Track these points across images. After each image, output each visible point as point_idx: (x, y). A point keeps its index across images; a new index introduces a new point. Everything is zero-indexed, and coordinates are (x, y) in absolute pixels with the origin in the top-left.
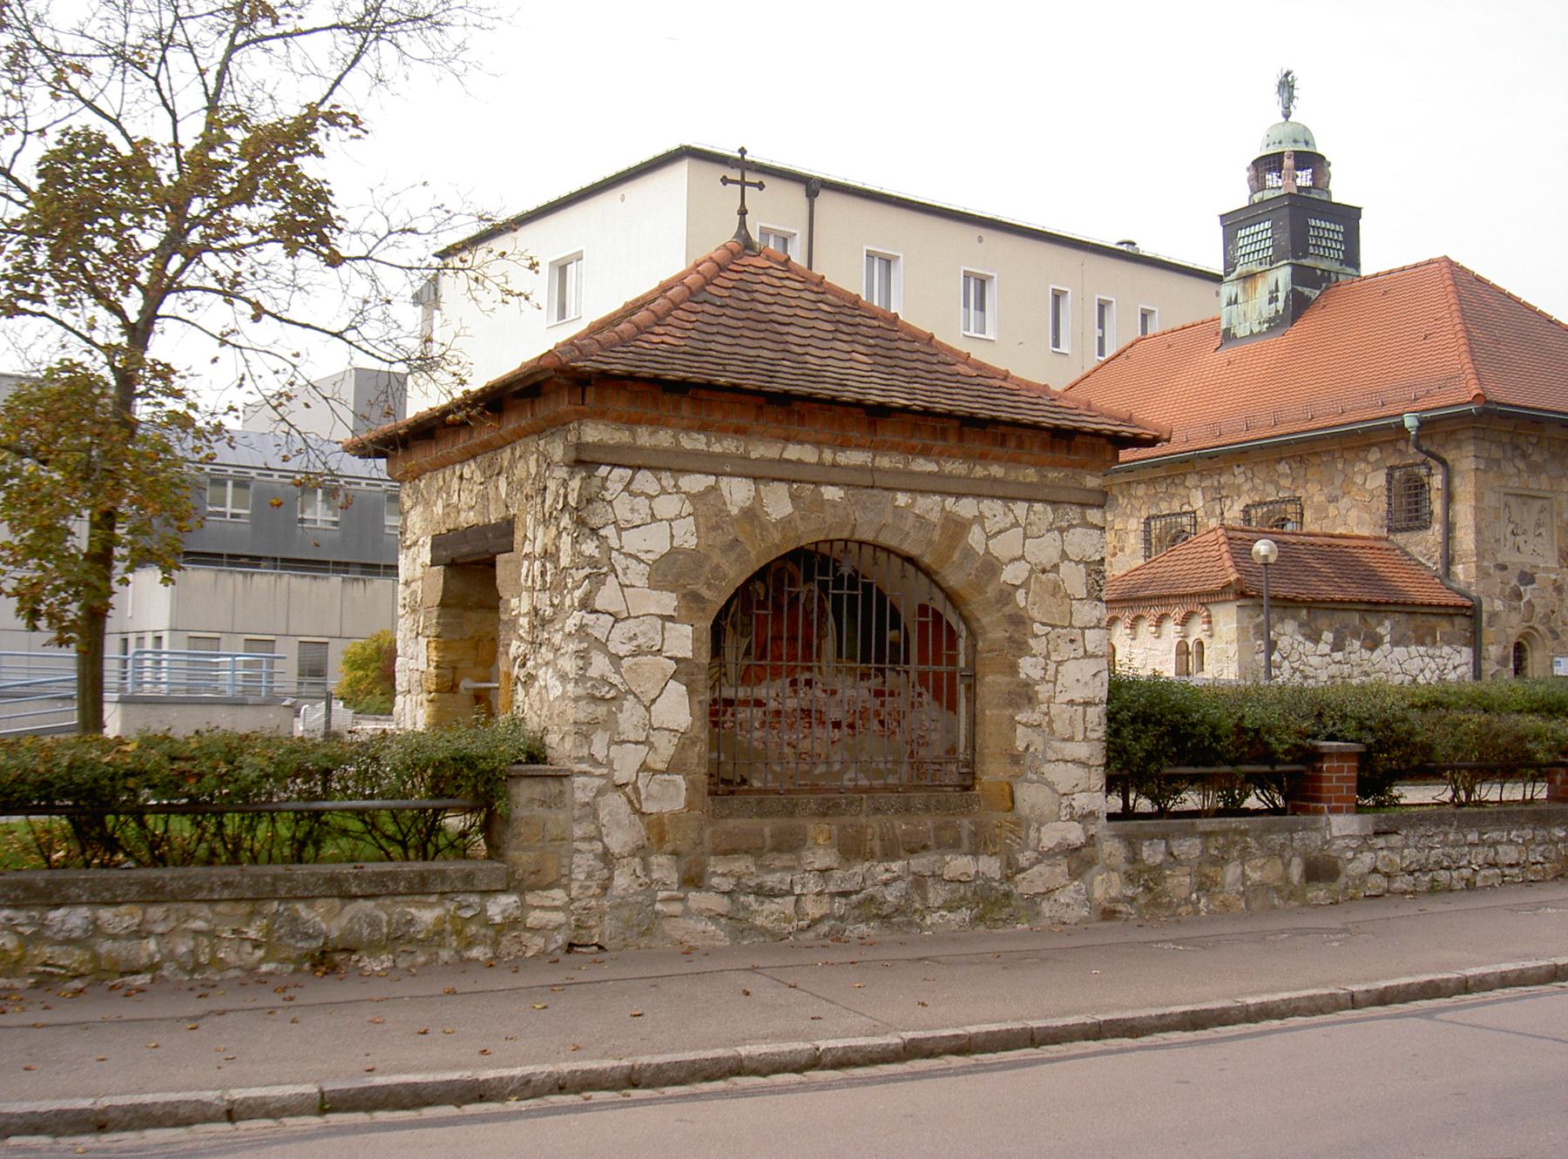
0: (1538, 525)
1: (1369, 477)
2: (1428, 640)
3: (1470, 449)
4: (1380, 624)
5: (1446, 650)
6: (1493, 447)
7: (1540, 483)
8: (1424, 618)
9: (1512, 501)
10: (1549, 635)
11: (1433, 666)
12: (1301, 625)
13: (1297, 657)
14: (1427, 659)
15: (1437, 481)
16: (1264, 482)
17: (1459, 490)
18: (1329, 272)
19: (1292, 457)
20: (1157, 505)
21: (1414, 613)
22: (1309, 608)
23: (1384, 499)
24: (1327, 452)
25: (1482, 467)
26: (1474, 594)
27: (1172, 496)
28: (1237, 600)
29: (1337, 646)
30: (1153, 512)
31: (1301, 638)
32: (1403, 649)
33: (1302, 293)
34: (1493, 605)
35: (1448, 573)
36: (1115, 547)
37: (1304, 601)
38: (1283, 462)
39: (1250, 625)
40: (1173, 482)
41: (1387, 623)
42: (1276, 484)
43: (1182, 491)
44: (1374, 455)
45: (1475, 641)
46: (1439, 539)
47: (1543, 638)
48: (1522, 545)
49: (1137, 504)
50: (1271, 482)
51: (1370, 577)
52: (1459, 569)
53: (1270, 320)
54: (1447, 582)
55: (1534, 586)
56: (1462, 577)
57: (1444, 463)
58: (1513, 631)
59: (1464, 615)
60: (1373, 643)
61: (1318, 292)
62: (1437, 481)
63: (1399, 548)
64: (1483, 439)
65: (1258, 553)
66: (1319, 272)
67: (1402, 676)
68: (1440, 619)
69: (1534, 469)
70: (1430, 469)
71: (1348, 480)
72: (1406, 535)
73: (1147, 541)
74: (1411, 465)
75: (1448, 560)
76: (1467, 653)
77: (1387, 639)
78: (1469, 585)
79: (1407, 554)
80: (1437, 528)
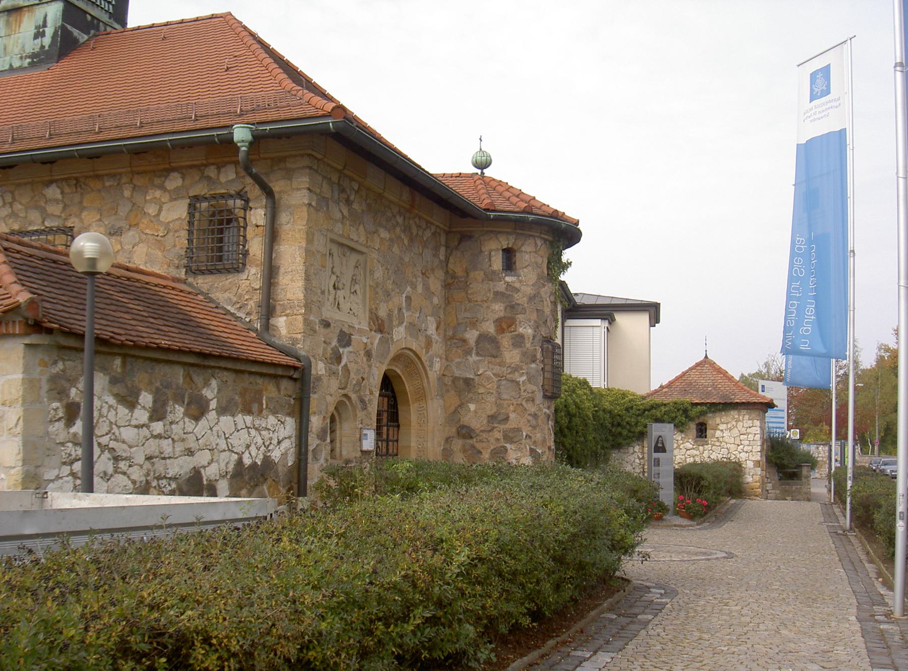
0: (354, 281)
1: (165, 207)
2: (255, 407)
3: (303, 180)
4: (207, 384)
5: (272, 420)
6: (325, 185)
7: (358, 236)
8: (252, 379)
9: (335, 249)
10: (359, 405)
11: (260, 441)
12: (114, 381)
13: (106, 429)
14: (253, 432)
15: (258, 216)
16: (27, 208)
17: (286, 228)
18: (99, 20)
21: (242, 372)
22: (124, 356)
23: (184, 234)
24: (113, 176)
25: (314, 204)
26: (303, 353)
28: (27, 334)
29: (157, 414)
31: (112, 401)
32: (229, 417)
33: (71, 33)
34: (319, 368)
35: (267, 326)
37: (122, 345)
38: (54, 185)
39: (43, 376)
41: (214, 383)
44: (174, 182)
45: (301, 412)
46: (257, 285)
47: (354, 408)
48: (341, 300)
50: (37, 207)
51: (186, 323)
52: (281, 322)
53: (33, 56)
54: (267, 337)
55: (350, 349)
56: (284, 332)
57: (269, 193)
59: (291, 378)
60: (198, 410)
61: (86, 37)
62: (258, 216)
63: (202, 293)
64: (316, 171)
65: (80, 253)
66: (89, 18)
67: (227, 453)
68: (267, 381)
69: (355, 219)
70: (247, 201)
71: (137, 209)
72: (210, 279)
74: (222, 196)
75: (269, 310)
76: (290, 424)
77: (213, 404)
78: (295, 341)
79: (211, 300)
80: (253, 276)
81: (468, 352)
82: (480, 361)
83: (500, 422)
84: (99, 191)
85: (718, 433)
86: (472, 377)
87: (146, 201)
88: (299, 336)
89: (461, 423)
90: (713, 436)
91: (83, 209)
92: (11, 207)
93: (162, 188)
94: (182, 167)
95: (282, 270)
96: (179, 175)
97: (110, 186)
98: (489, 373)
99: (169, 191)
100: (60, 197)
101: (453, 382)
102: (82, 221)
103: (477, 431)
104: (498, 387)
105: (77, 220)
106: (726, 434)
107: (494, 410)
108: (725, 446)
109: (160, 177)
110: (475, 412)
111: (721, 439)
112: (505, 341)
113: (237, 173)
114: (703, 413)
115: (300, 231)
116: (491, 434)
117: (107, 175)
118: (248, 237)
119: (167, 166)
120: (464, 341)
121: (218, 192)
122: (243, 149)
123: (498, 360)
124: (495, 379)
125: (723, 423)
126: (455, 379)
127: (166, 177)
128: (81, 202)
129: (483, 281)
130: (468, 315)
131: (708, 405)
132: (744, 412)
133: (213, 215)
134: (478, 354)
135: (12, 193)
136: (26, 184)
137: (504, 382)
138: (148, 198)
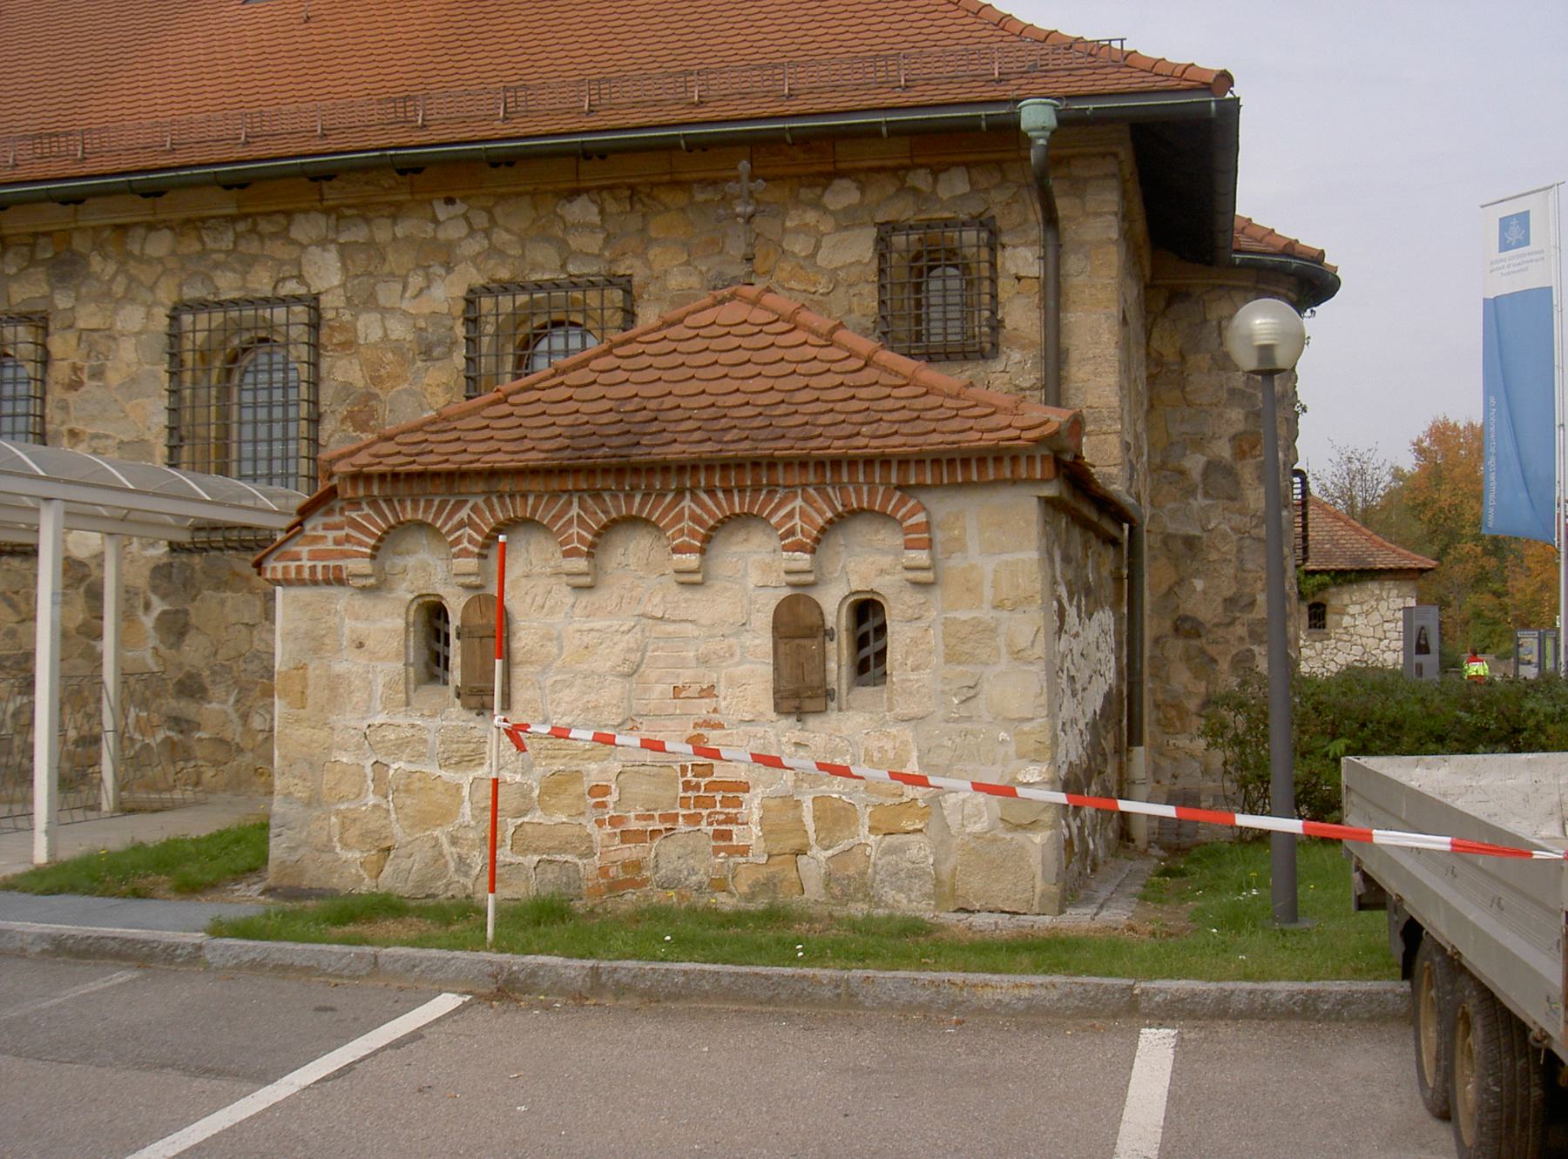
1: (826, 241)
16: (523, 240)
17: (1075, 281)
19: (610, 188)
20: (207, 278)
27: (249, 262)
30: (194, 292)
36: (76, 369)
38: (585, 197)
40: (253, 230)
42: (562, 245)
43: (279, 249)
44: (843, 195)
49: (145, 274)
50: (549, 239)
57: (1051, 220)
70: (994, 234)
73: (175, 357)
74: (947, 224)
81: (1190, 492)
82: (1212, 506)
83: (1242, 610)
84: (682, 210)
85: (1347, 621)
86: (1198, 533)
87: (784, 230)
88: (1114, 470)
89: (1181, 612)
90: (1339, 625)
91: (649, 242)
92: (487, 233)
93: (817, 205)
94: (858, 170)
95: (1074, 355)
96: (854, 185)
97: (706, 202)
98: (1225, 527)
99: (833, 213)
100: (597, 220)
101: (1165, 543)
102: (648, 264)
103: (1208, 626)
104: (1240, 550)
105: (637, 263)
106: (1360, 621)
107: (1234, 589)
108: (1359, 642)
109: (810, 186)
110: (1204, 592)
111: (1352, 630)
112: (1247, 471)
113: (972, 183)
114: (1322, 587)
115: (1105, 287)
116: (1231, 629)
117: (700, 181)
118: (1002, 296)
119: (830, 168)
120: (1182, 473)
121: (935, 216)
122: (1042, 142)
123: (1237, 505)
124: (1235, 538)
125: (1354, 603)
126: (1167, 539)
127: (825, 188)
128: (643, 230)
129: (1209, 370)
130: (1186, 428)
131: (1333, 574)
132: (1389, 584)
133: (917, 257)
134: (1206, 495)
135: (489, 211)
136: (519, 195)
137: (1247, 542)
138: (789, 224)
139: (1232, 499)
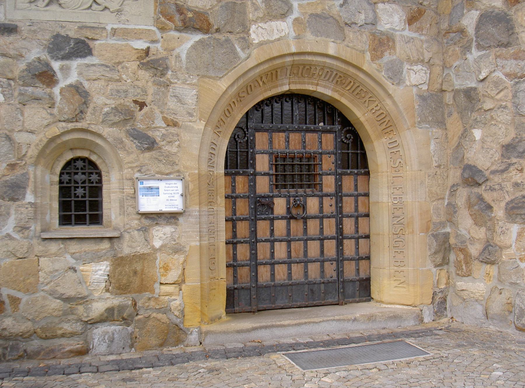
55: (88, 60)
58: (34, 139)
81: (467, 49)
86: (473, 85)
89: (466, 162)
98: (499, 74)
103: (487, 173)
104: (515, 96)
107: (512, 134)
110: (483, 141)
116: (505, 175)
120: (462, 31)
123: (511, 50)
124: (509, 83)
134: (479, 47)
139: (507, 45)
